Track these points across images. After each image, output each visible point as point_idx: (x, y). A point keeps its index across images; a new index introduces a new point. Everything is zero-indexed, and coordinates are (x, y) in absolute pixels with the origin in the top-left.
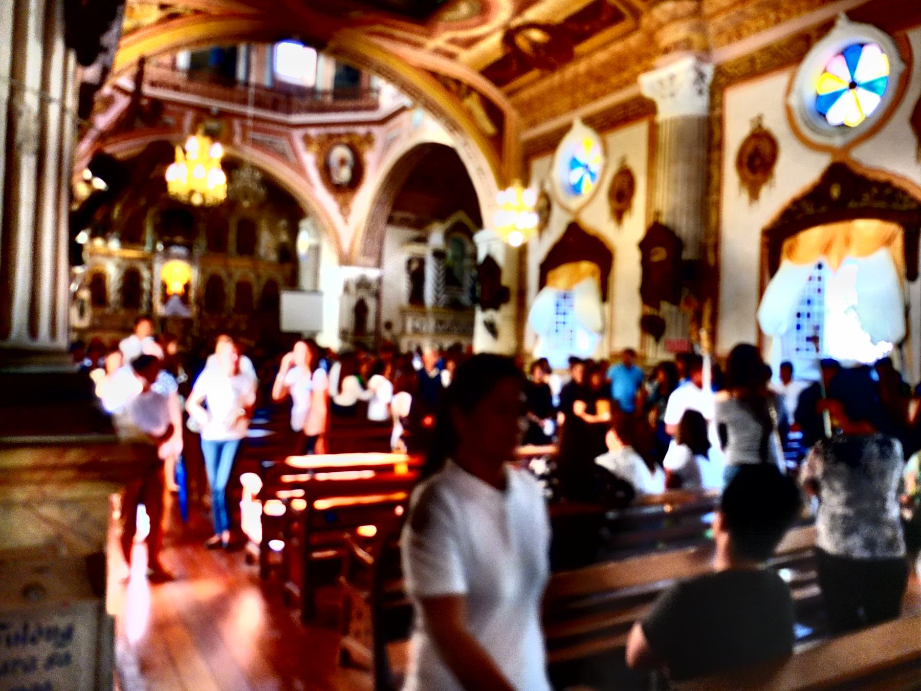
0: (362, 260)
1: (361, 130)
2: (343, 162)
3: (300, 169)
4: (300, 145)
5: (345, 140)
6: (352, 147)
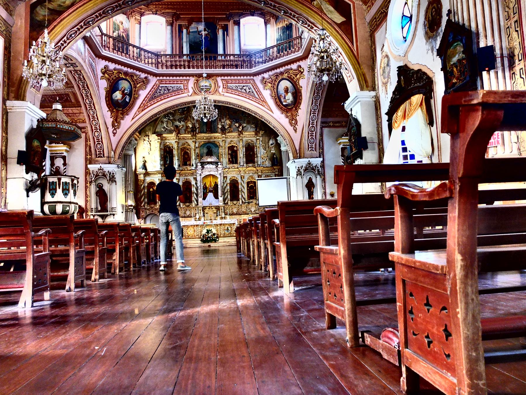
0: (308, 153)
1: (294, 66)
2: (287, 90)
3: (263, 101)
4: (260, 86)
5: (285, 76)
6: (290, 79)
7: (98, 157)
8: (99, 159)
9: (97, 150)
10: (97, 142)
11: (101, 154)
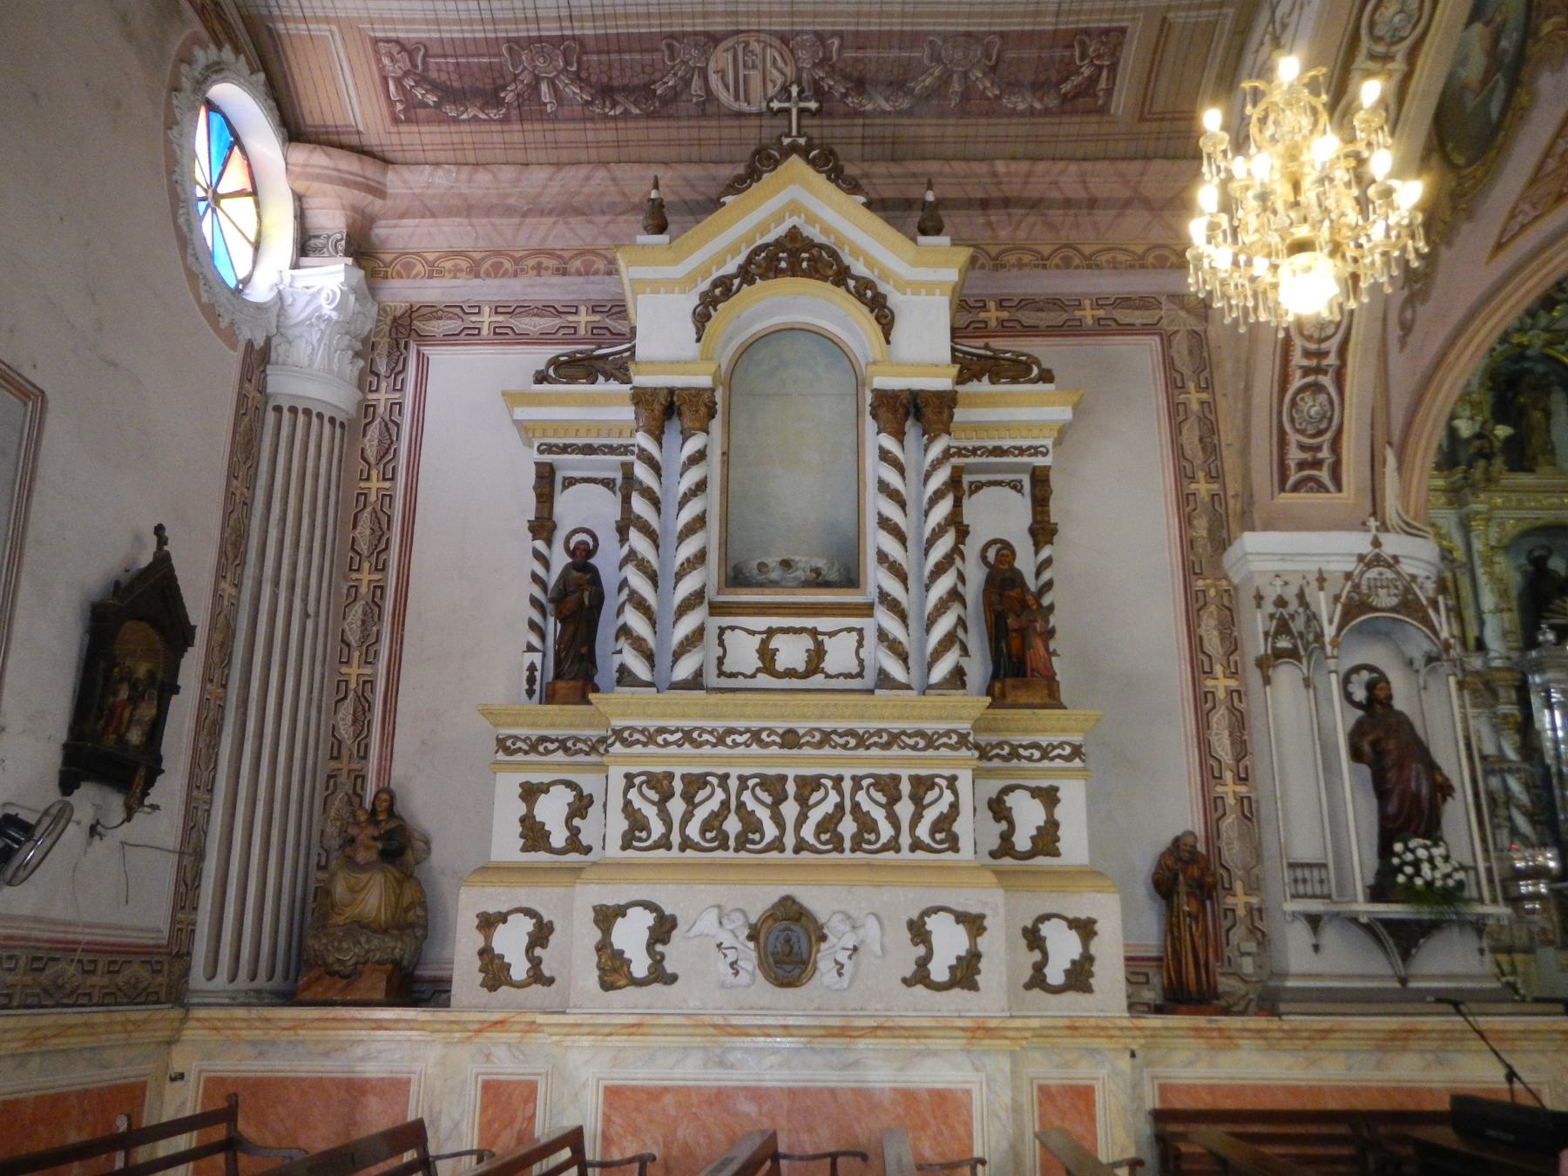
7: (1296, 488)
8: (1302, 497)
9: (1293, 438)
10: (1307, 371)
11: (1317, 464)
